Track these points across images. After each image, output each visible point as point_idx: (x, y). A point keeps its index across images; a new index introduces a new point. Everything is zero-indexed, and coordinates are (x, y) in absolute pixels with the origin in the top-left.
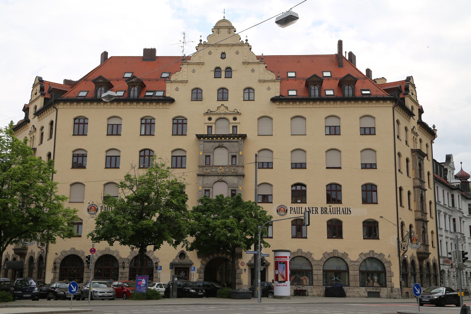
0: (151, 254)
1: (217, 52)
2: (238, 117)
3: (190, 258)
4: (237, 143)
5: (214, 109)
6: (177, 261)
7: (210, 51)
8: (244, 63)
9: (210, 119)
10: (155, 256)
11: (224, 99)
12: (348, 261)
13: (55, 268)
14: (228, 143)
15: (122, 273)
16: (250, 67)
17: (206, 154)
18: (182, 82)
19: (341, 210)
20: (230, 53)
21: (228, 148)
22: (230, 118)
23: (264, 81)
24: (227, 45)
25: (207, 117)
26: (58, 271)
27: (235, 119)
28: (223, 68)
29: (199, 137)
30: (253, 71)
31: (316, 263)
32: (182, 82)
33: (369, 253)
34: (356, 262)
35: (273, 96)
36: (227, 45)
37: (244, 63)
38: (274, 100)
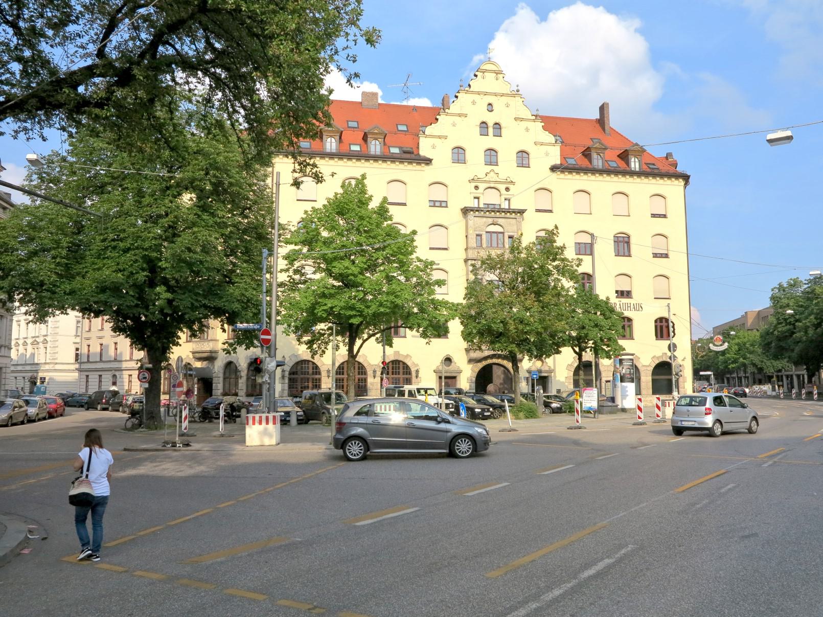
0: (408, 359)
1: (483, 101)
2: (511, 186)
3: (457, 365)
4: (514, 220)
5: (481, 175)
6: (441, 368)
7: (474, 101)
8: (516, 119)
9: (476, 188)
10: (413, 362)
11: (492, 164)
12: (639, 366)
13: (283, 377)
14: (503, 220)
15: (372, 384)
16: (524, 124)
17: (477, 233)
18: (440, 137)
19: (632, 306)
20: (498, 103)
21: (504, 226)
22: (502, 187)
23: (542, 144)
24: (496, 95)
25: (474, 184)
26: (287, 381)
27: (507, 189)
28: (491, 124)
29: (466, 211)
30: (527, 130)
31: (606, 369)
32: (440, 137)
33: (662, 356)
34: (648, 366)
35: (553, 163)
36: (496, 95)
37: (516, 119)
38: (554, 169)
